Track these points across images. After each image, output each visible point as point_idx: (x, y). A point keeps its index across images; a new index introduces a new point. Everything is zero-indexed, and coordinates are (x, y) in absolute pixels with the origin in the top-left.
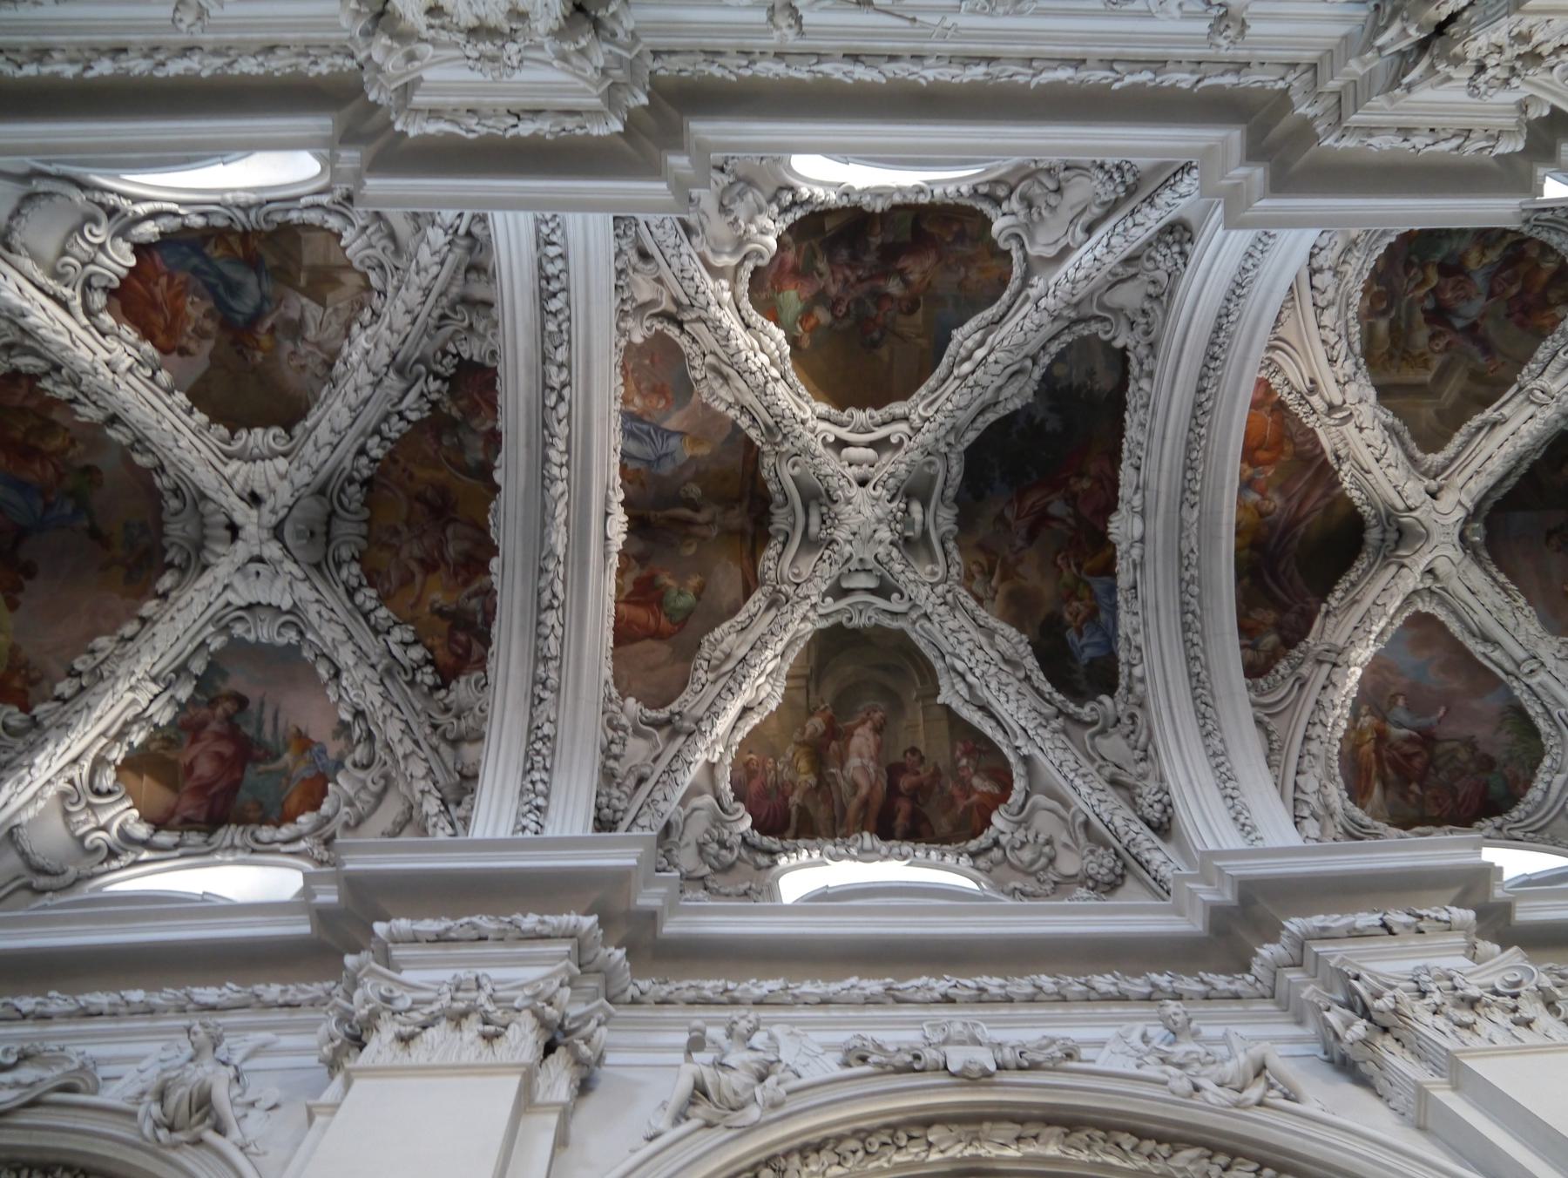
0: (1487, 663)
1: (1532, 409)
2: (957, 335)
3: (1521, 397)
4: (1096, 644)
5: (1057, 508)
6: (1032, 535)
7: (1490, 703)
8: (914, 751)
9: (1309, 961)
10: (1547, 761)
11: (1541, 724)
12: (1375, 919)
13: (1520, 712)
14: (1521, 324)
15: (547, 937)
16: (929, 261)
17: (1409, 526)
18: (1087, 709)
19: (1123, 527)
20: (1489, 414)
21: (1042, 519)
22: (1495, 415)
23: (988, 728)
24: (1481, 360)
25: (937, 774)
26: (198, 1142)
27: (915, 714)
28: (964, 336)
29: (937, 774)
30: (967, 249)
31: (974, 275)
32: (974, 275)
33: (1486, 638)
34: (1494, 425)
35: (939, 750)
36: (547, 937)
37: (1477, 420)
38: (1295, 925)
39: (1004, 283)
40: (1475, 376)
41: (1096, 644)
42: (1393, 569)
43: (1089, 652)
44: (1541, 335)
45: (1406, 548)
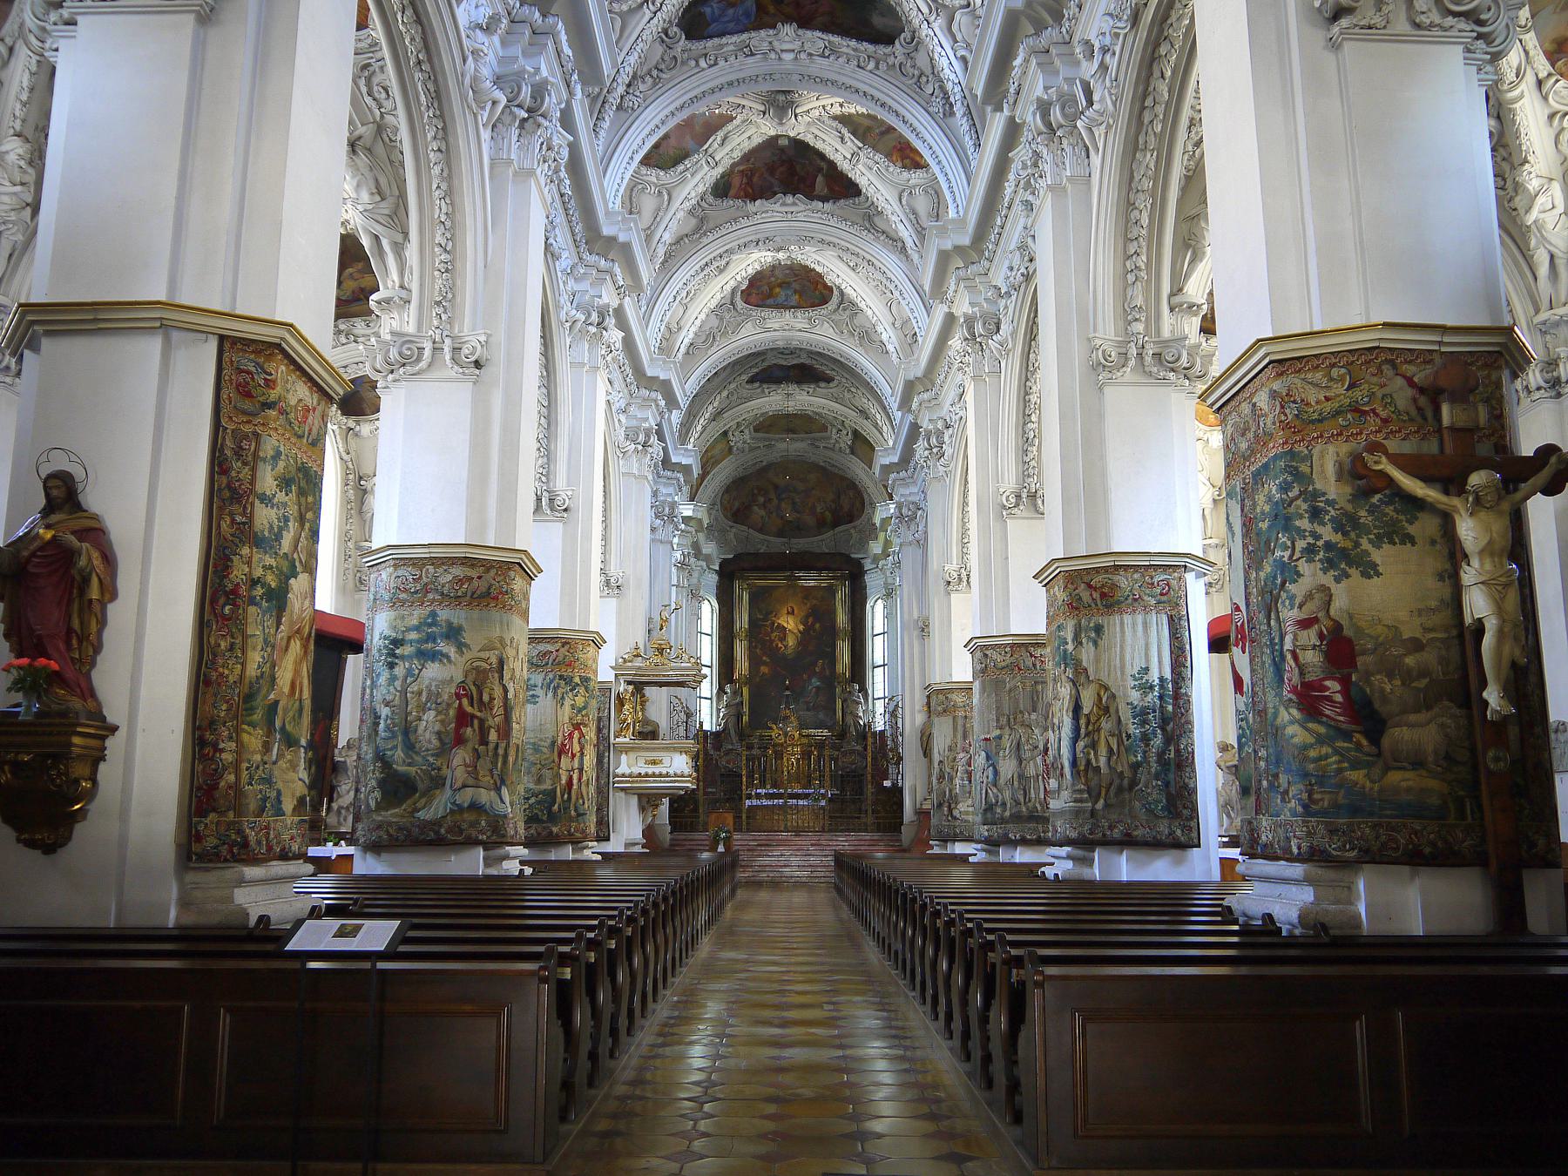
0: (711, 140)
1: (849, 157)
3: (856, 149)
4: (713, 12)
7: (689, 143)
9: (602, 275)
10: (662, 173)
11: (681, 168)
12: (621, 283)
13: (685, 156)
14: (895, 147)
15: (568, 86)
17: (787, 113)
18: (675, 29)
19: (788, 35)
20: (847, 135)
22: (846, 139)
24: (877, 131)
26: (475, 115)
33: (724, 141)
34: (842, 139)
36: (568, 86)
37: (845, 131)
38: (617, 270)
40: (869, 129)
41: (713, 12)
42: (762, 108)
43: (708, 10)
44: (888, 155)
45: (775, 111)
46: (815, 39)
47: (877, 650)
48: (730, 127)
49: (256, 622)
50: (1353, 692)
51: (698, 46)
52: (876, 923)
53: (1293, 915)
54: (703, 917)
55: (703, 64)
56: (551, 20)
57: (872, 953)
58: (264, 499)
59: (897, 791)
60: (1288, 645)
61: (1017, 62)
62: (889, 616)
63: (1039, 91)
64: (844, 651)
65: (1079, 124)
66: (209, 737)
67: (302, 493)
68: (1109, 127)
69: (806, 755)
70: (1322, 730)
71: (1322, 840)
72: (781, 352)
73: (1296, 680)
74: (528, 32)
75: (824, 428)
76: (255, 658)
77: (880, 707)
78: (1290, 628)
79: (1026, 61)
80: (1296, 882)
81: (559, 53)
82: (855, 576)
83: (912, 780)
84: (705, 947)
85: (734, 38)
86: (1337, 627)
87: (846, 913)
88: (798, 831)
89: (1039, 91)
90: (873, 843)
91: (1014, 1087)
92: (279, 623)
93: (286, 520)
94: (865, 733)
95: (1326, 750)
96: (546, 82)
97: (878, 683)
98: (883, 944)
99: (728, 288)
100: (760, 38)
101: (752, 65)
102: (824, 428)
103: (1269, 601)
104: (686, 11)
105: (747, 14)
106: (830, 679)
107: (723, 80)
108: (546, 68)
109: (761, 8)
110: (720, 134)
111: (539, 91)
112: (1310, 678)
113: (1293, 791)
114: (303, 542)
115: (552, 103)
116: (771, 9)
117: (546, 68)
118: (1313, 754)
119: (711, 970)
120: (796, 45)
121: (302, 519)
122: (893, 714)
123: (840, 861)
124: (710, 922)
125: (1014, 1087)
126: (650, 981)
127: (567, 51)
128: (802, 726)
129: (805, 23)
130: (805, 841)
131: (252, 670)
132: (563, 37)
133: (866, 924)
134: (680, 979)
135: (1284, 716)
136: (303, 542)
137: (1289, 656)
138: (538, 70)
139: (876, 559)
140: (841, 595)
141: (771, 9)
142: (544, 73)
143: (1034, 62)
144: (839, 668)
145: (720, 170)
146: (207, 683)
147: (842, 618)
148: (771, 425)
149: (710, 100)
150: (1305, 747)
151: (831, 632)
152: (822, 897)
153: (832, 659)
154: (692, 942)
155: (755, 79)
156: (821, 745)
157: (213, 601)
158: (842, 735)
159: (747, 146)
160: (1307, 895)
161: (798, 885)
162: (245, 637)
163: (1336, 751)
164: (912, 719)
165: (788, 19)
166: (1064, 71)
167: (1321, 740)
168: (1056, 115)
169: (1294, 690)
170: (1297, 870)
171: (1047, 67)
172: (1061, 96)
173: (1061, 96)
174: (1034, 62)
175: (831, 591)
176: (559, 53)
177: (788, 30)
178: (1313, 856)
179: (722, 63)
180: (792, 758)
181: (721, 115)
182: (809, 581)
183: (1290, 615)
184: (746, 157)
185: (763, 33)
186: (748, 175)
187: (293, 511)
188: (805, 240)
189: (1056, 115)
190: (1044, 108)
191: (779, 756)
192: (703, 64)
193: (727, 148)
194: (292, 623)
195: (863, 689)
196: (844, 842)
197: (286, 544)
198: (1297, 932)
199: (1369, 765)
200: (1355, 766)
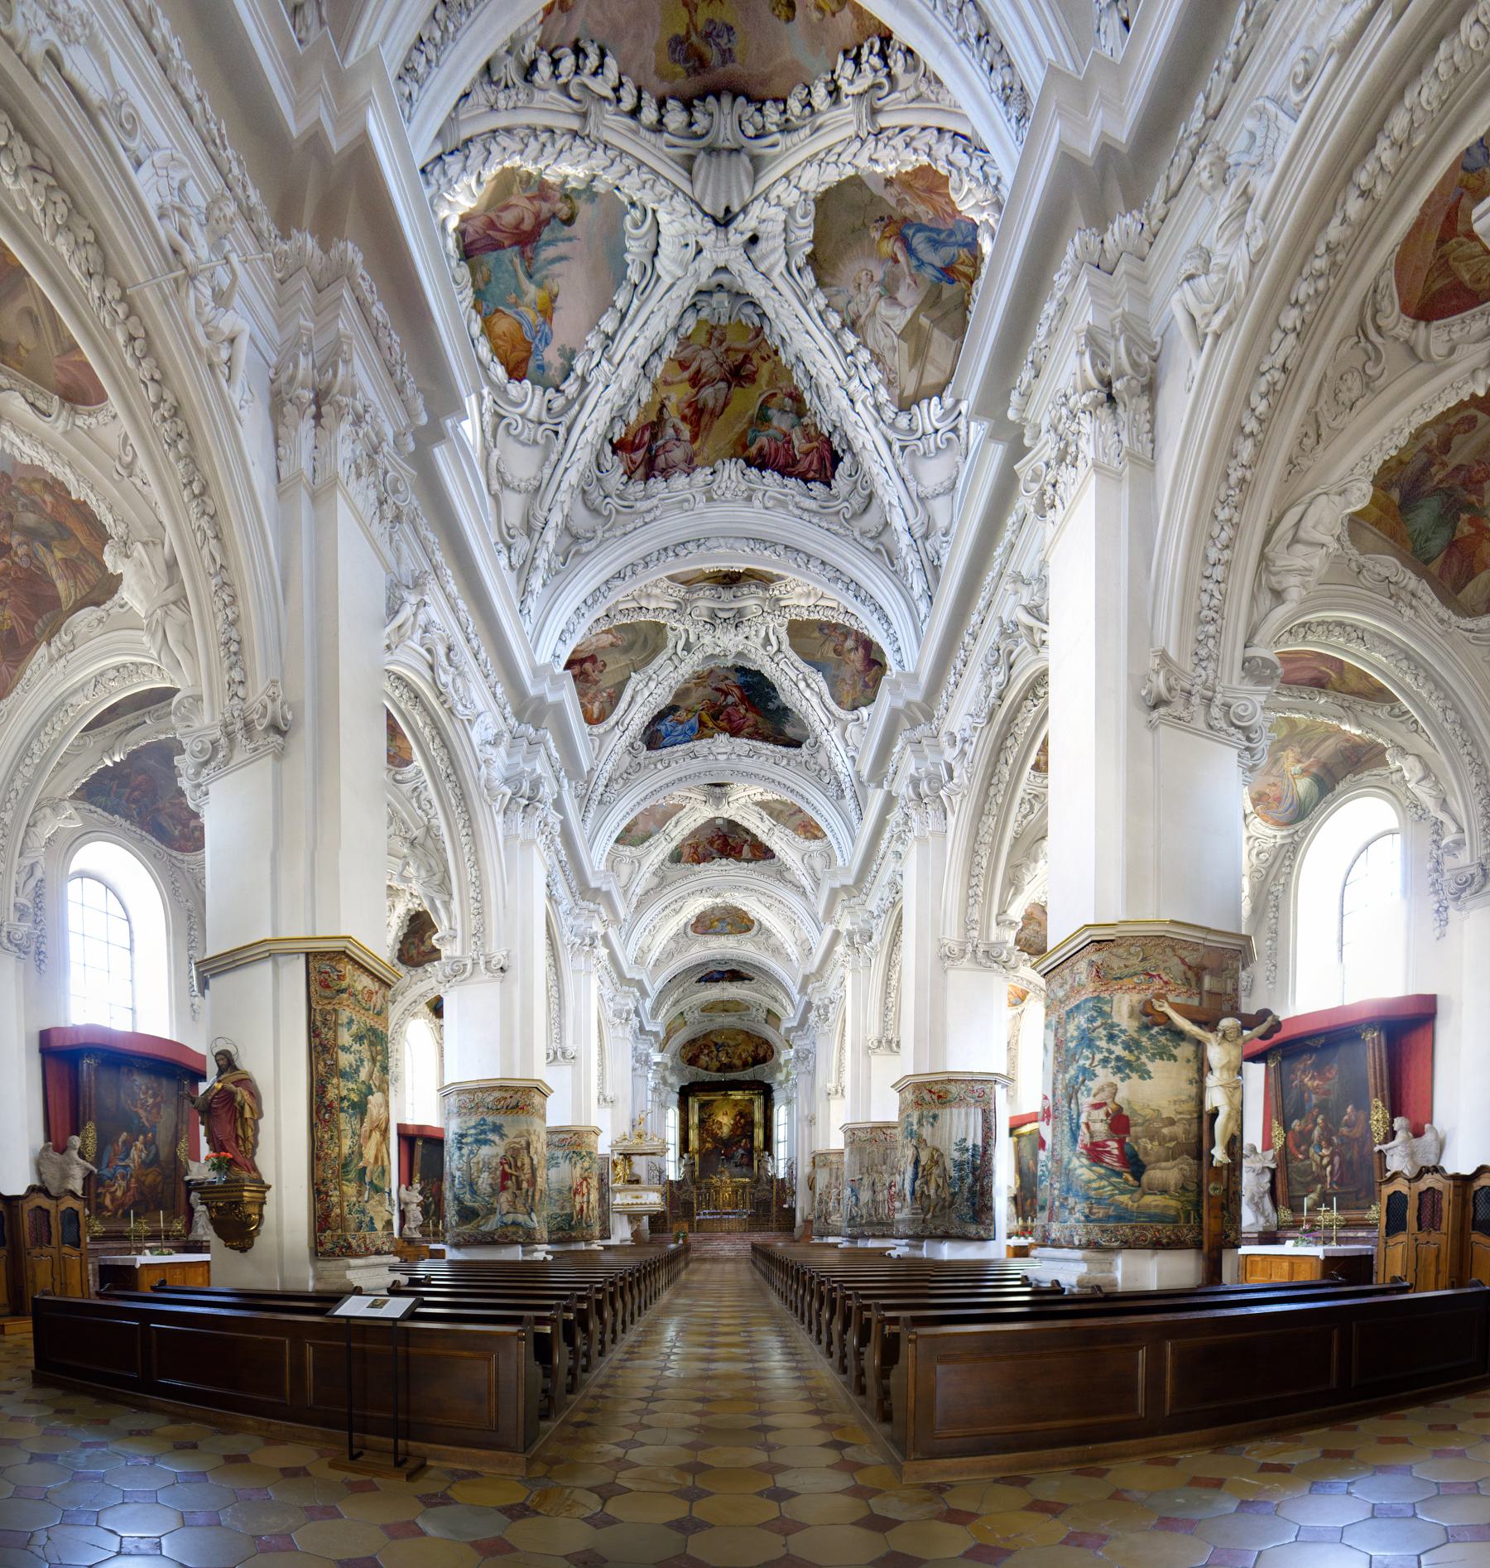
2: (819, 677)
5: (730, 699)
6: (717, 689)
8: (605, 665)
16: (859, 665)
19: (722, 742)
21: (726, 694)
23: (623, 705)
25: (596, 682)
27: (624, 660)
28: (819, 682)
29: (596, 682)
30: (859, 687)
31: (847, 688)
32: (847, 688)
35: (607, 680)
39: (839, 704)
43: (663, 728)
46: (742, 744)
47: (780, 1132)
48: (681, 813)
49: (346, 1122)
50: (1126, 1148)
51: (655, 754)
52: (778, 1284)
53: (1074, 1281)
54: (663, 1281)
55: (660, 766)
56: (541, 732)
57: (775, 1300)
58: (343, 1048)
59: (792, 1211)
60: (1083, 1119)
61: (896, 750)
62: (789, 1114)
63: (912, 770)
64: (759, 1134)
65: (942, 793)
66: (322, 1188)
67: (371, 1044)
68: (964, 796)
69: (735, 1192)
70: (1102, 1171)
71: (1096, 1235)
72: (719, 962)
73: (1087, 1140)
74: (525, 744)
75: (748, 1008)
76: (347, 1144)
77: (782, 1164)
78: (1085, 1109)
79: (903, 748)
80: (1076, 1261)
81: (549, 757)
82: (766, 1092)
83: (802, 1205)
84: (665, 1297)
85: (683, 747)
86: (1120, 1109)
87: (758, 1276)
88: (729, 1232)
89: (912, 770)
90: (776, 1237)
91: (885, 1393)
92: (362, 1122)
93: (362, 1061)
94: (772, 1180)
95: (1104, 1183)
96: (540, 777)
97: (781, 1151)
98: (782, 1295)
99: (682, 923)
100: (701, 746)
101: (696, 765)
102: (748, 1008)
103: (1072, 1095)
104: (648, 727)
105: (692, 729)
106: (750, 1151)
107: (674, 777)
108: (540, 767)
109: (702, 723)
110: (674, 819)
111: (536, 785)
112: (1096, 1140)
113: (1078, 1207)
114: (376, 1074)
115: (547, 791)
116: (710, 724)
117: (540, 767)
118: (1094, 1185)
119: (668, 1311)
120: (729, 749)
121: (374, 1060)
122: (790, 1167)
123: (755, 1248)
124: (669, 1283)
125: (885, 1393)
126: (628, 1315)
127: (556, 754)
128: (732, 1176)
129: (735, 732)
130: (732, 1237)
131: (346, 1150)
132: (552, 744)
133: (771, 1283)
134: (648, 1315)
135: (1075, 1163)
136: (376, 1074)
137: (1083, 1127)
138: (534, 770)
139: (781, 1083)
140: (758, 1104)
141: (710, 724)
142: (539, 770)
143: (909, 749)
144: (756, 1144)
145: (674, 844)
146: (319, 1159)
147: (758, 1116)
148: (710, 1008)
149: (665, 792)
150: (1090, 1182)
151: (751, 1124)
152: (743, 1266)
153: (751, 1138)
154: (656, 1294)
155: (698, 775)
156: (744, 1186)
157: (318, 1112)
158: (758, 1181)
159: (694, 826)
160: (1083, 1268)
161: (728, 1260)
162: (339, 1131)
163: (1111, 1184)
164: (803, 1170)
165: (723, 730)
166: (931, 757)
167: (1101, 1177)
168: (924, 788)
169: (1085, 1147)
170: (1078, 1254)
171: (918, 754)
172: (928, 774)
173: (928, 774)
174: (909, 749)
175: (751, 1101)
176: (549, 757)
177: (723, 739)
178: (1091, 1245)
179: (673, 765)
180: (726, 1194)
181: (674, 805)
182: (737, 1096)
183: (1085, 1101)
184: (693, 834)
185: (704, 741)
186: (695, 847)
187: (366, 1055)
188: (736, 888)
189: (924, 788)
190: (915, 782)
191: (717, 1192)
192: (660, 766)
193: (679, 829)
194: (372, 1122)
195: (771, 1154)
196: (758, 1238)
197: (363, 1074)
198: (1075, 1290)
199: (1132, 1192)
200: (1122, 1192)
